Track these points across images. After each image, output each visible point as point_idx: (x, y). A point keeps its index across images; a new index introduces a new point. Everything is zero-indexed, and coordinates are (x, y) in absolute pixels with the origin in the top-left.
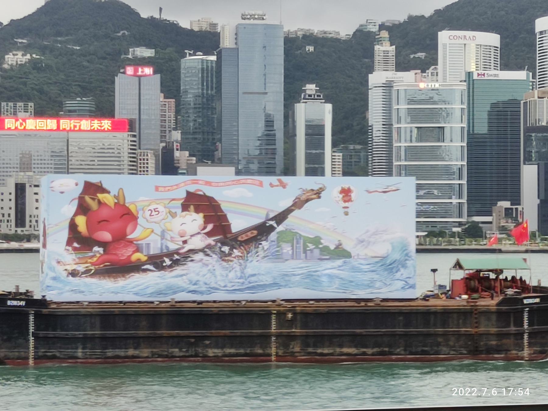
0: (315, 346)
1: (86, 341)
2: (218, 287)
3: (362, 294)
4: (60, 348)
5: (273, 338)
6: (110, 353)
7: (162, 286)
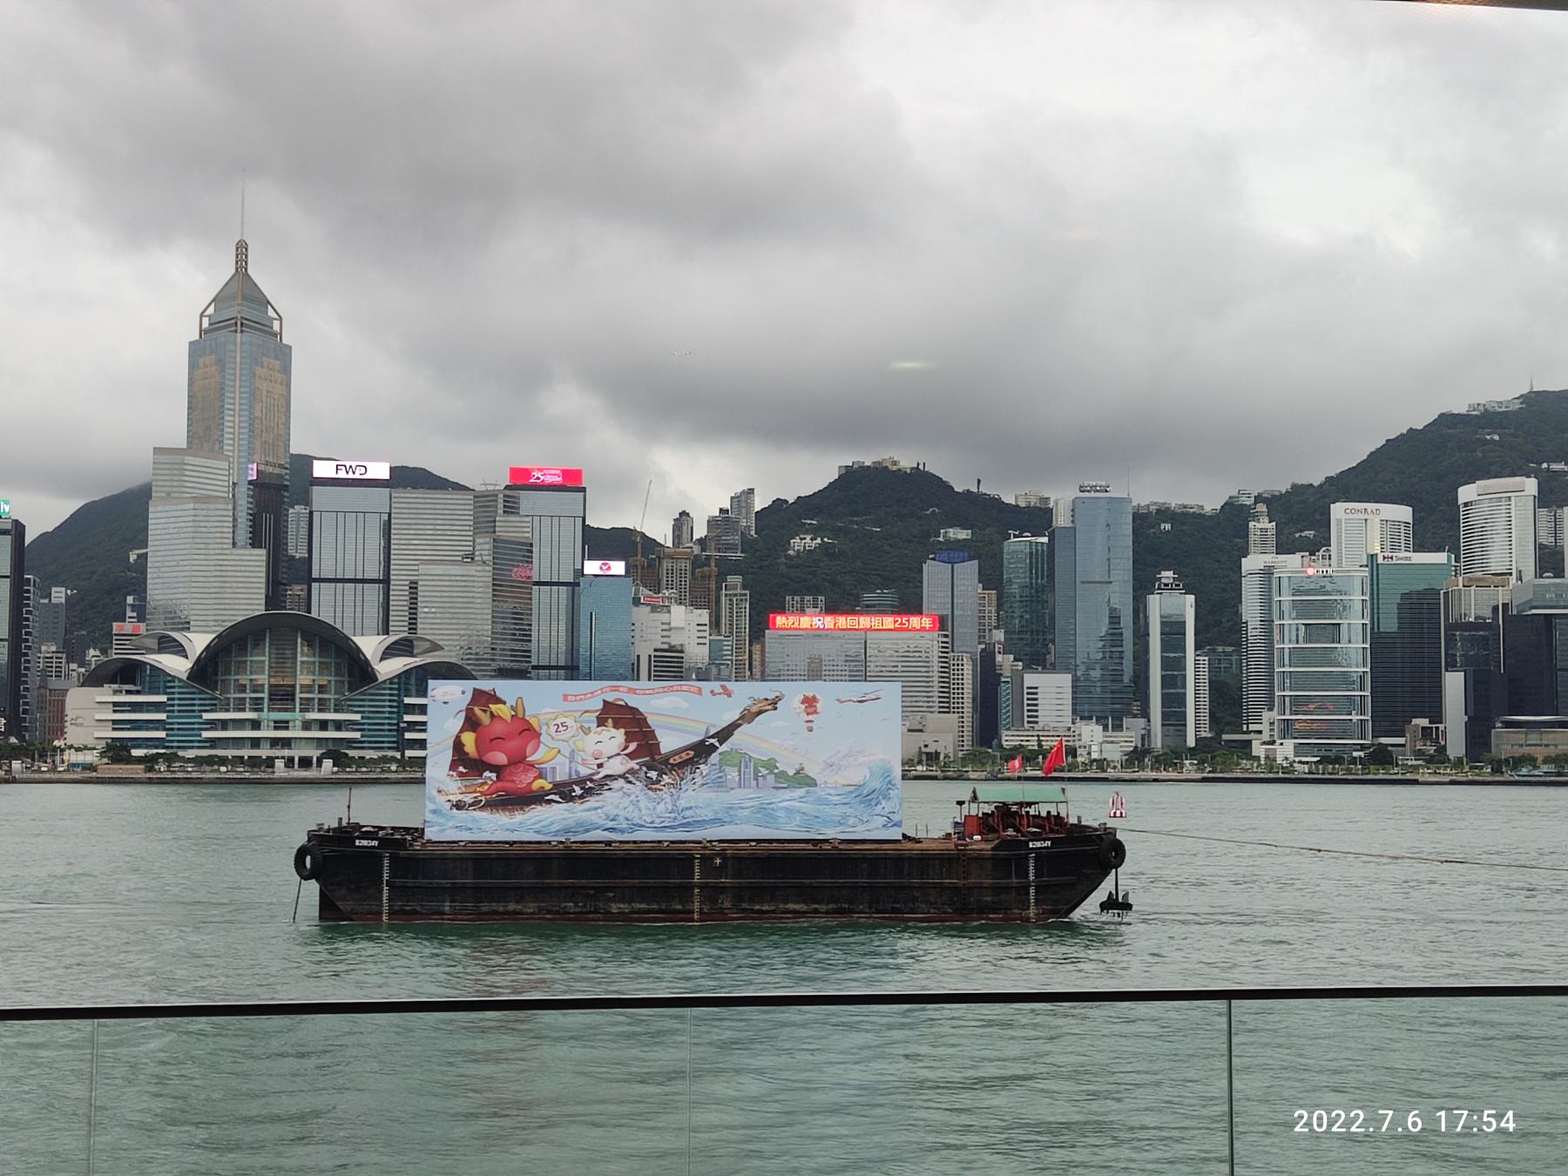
0: (751, 900)
1: (454, 892)
2: (643, 823)
3: (831, 833)
4: (422, 901)
5: (697, 890)
6: (485, 907)
7: (570, 822)
